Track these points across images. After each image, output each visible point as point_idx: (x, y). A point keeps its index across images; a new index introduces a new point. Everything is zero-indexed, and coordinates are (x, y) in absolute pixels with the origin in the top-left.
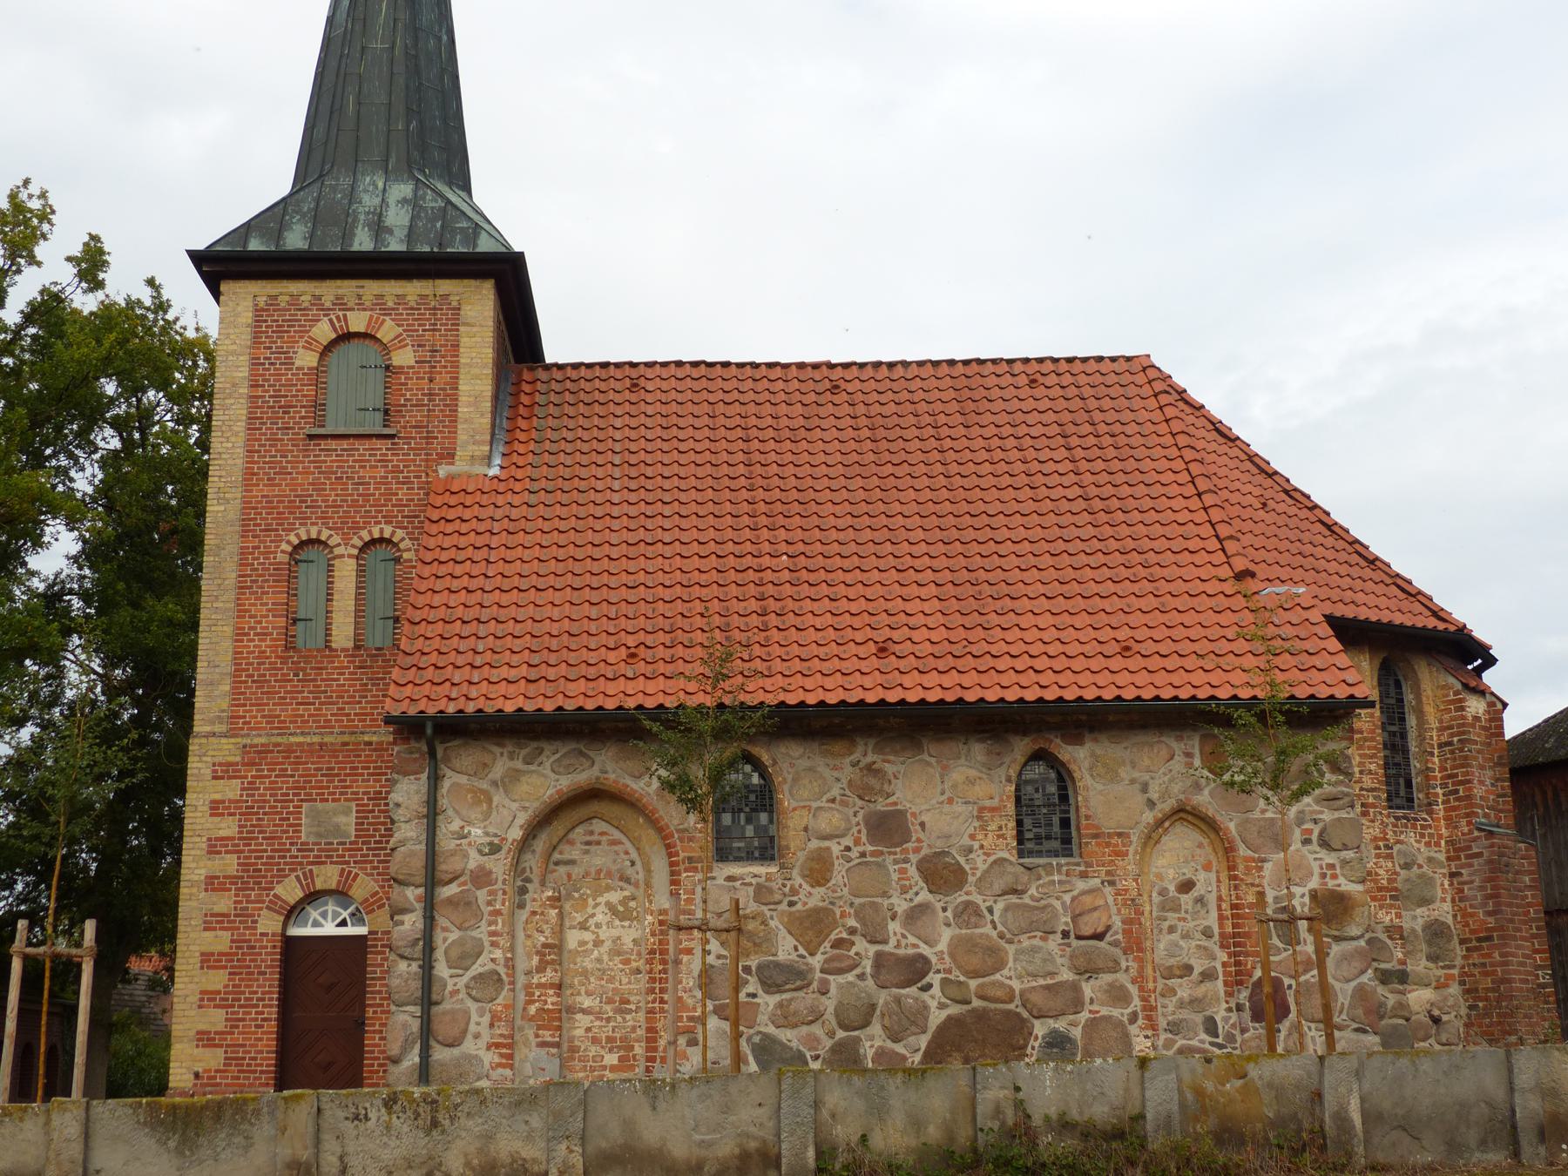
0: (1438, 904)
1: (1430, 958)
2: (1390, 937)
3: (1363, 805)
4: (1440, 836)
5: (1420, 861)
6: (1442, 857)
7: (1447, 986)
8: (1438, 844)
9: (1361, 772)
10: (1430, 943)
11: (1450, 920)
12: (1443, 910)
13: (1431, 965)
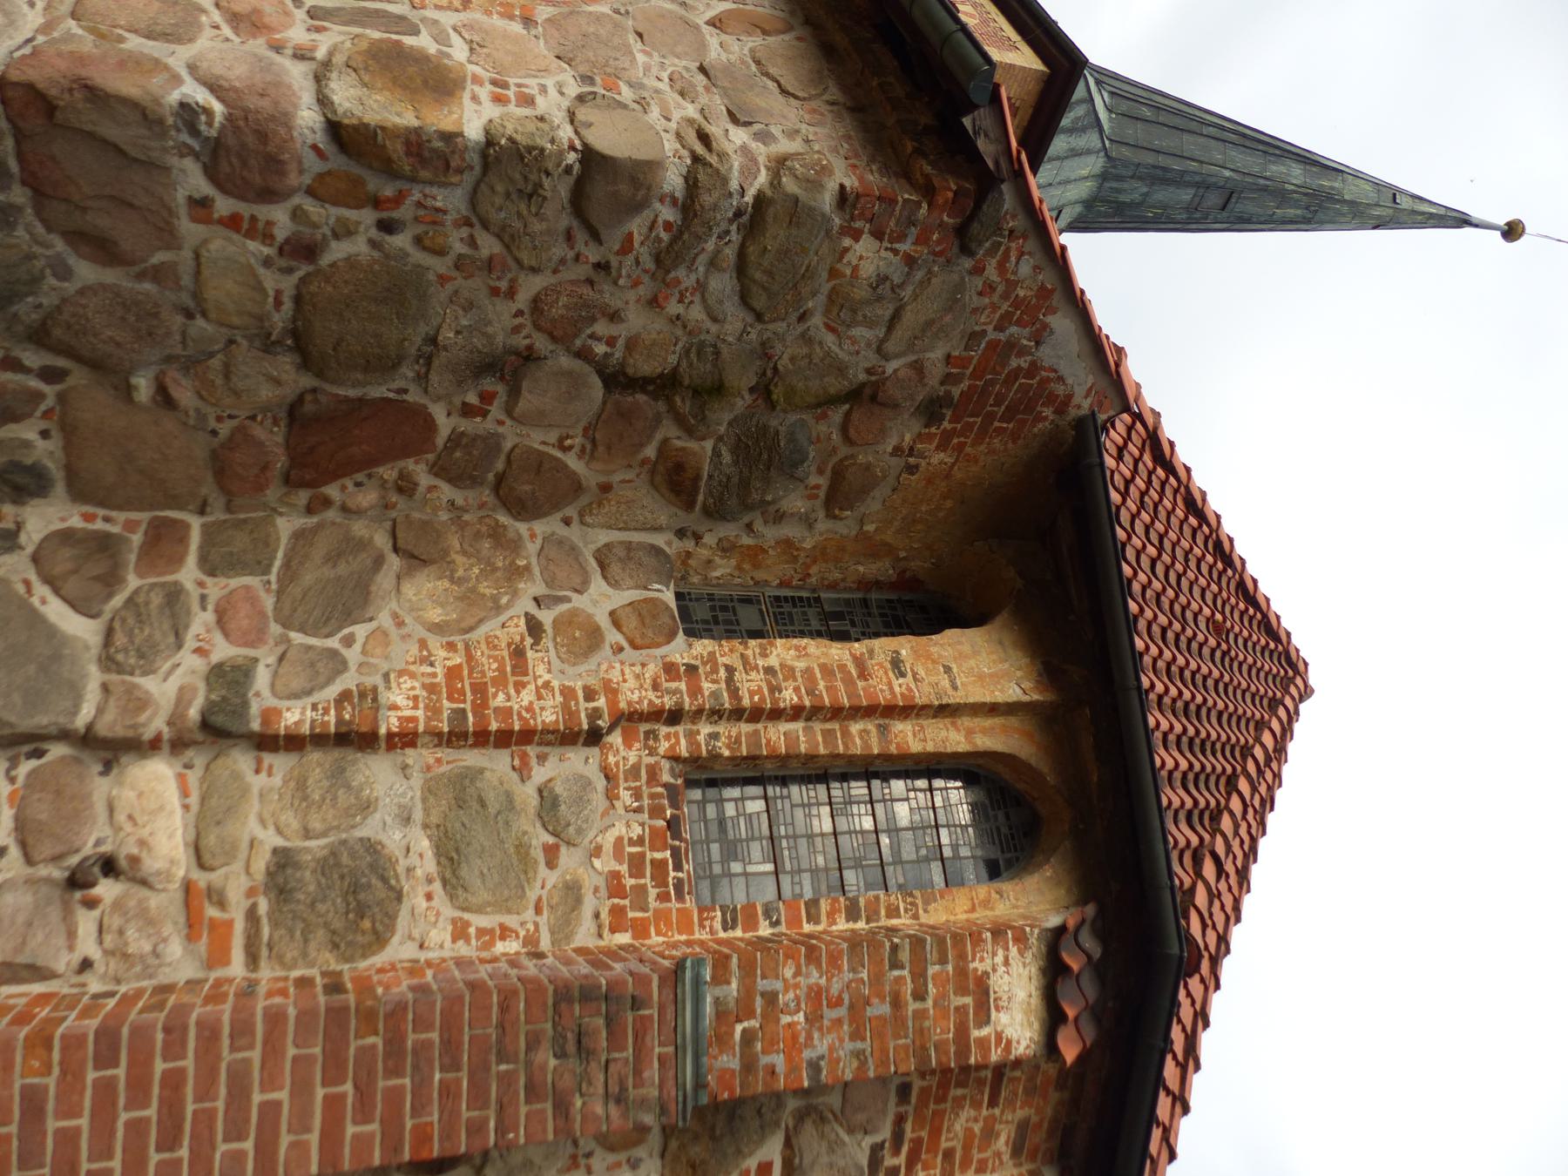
0: (449, 912)
1: (283, 860)
2: (345, 696)
3: (692, 669)
4: (640, 930)
5: (569, 859)
6: (584, 936)
7: (191, 935)
8: (618, 920)
9: (769, 670)
10: (328, 864)
11: (399, 950)
12: (428, 935)
13: (260, 864)
